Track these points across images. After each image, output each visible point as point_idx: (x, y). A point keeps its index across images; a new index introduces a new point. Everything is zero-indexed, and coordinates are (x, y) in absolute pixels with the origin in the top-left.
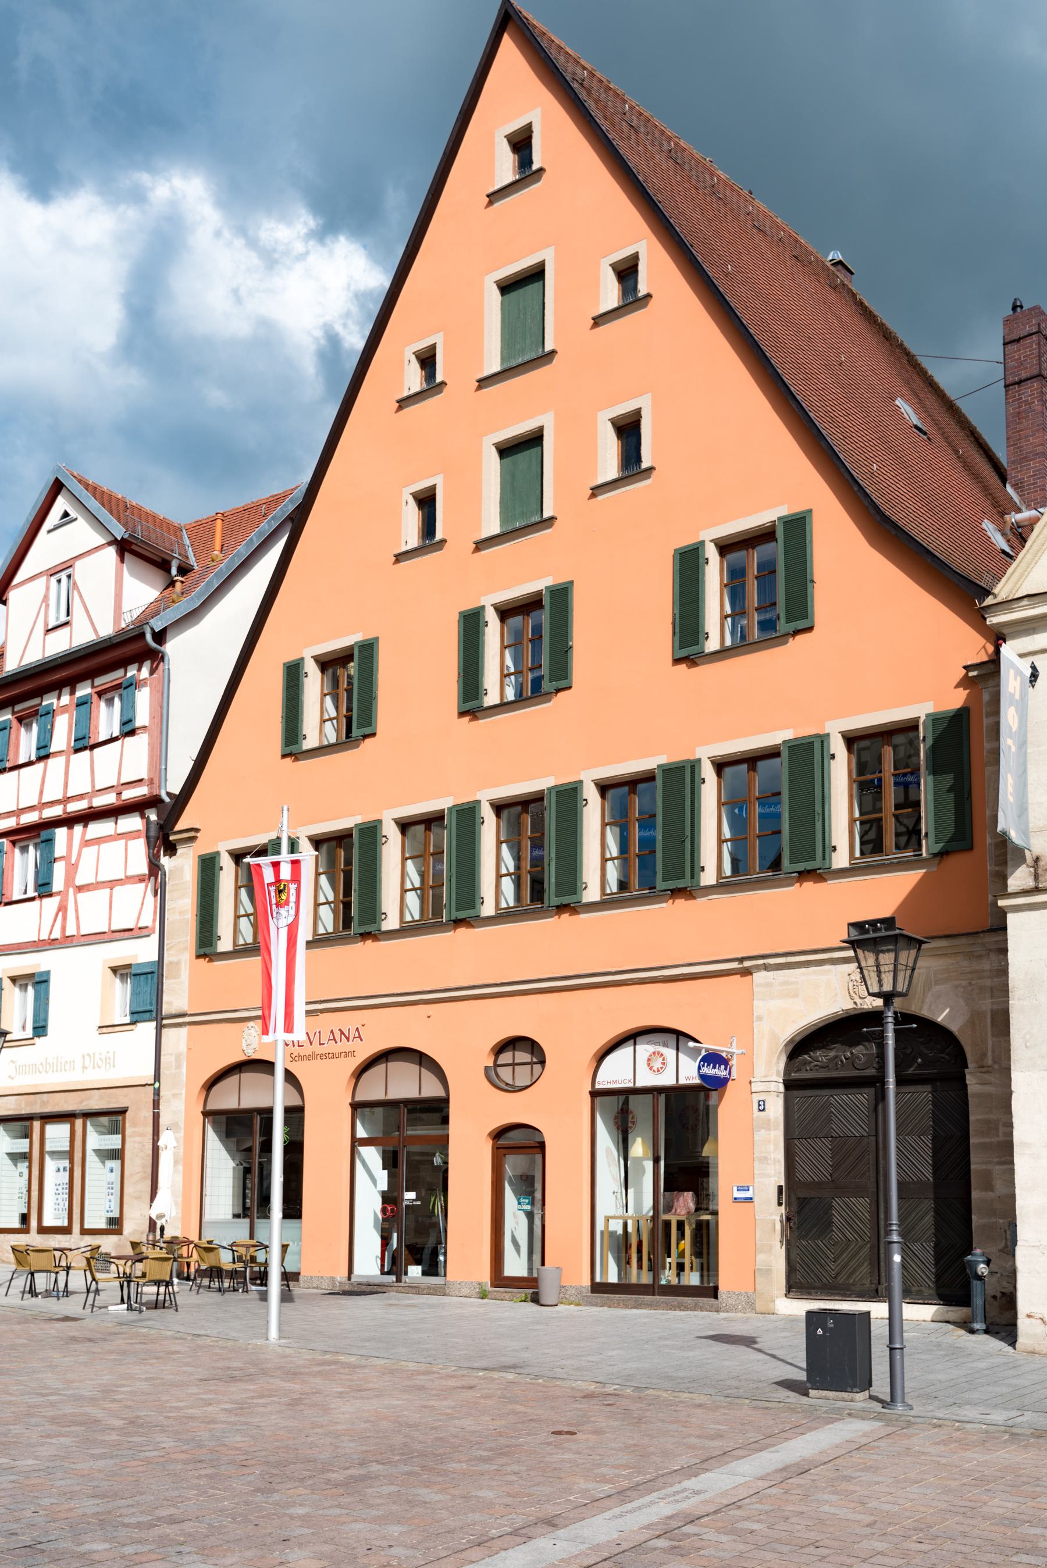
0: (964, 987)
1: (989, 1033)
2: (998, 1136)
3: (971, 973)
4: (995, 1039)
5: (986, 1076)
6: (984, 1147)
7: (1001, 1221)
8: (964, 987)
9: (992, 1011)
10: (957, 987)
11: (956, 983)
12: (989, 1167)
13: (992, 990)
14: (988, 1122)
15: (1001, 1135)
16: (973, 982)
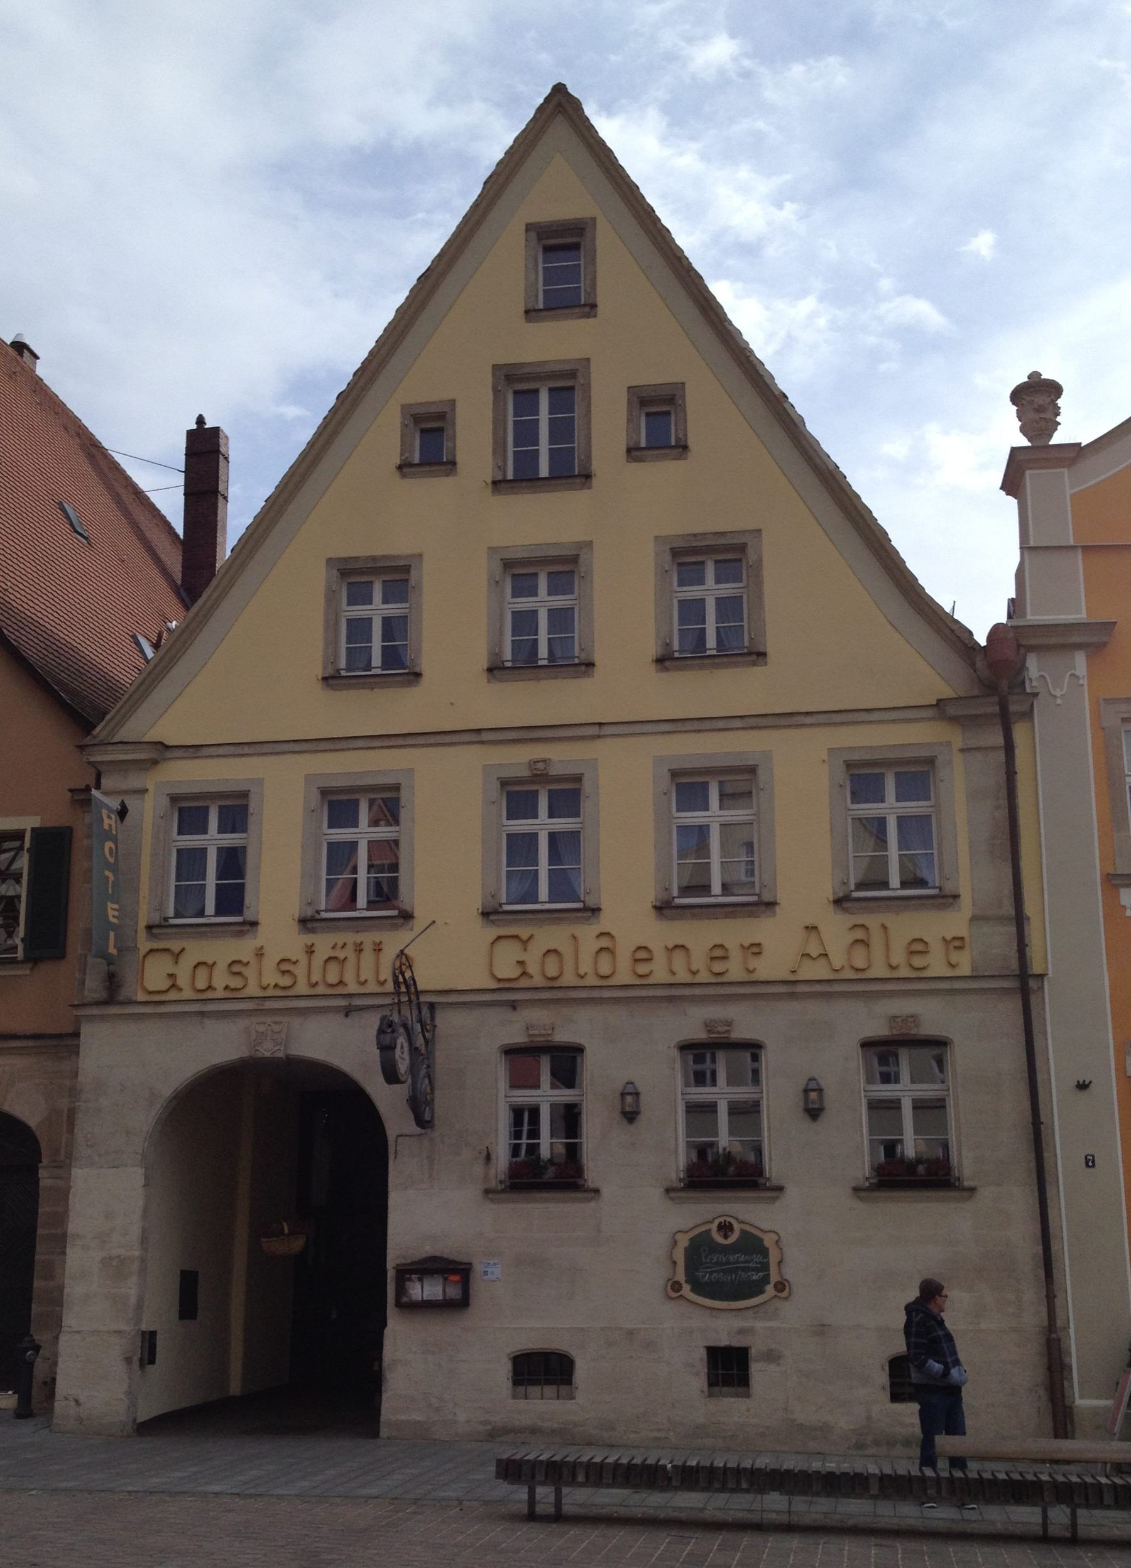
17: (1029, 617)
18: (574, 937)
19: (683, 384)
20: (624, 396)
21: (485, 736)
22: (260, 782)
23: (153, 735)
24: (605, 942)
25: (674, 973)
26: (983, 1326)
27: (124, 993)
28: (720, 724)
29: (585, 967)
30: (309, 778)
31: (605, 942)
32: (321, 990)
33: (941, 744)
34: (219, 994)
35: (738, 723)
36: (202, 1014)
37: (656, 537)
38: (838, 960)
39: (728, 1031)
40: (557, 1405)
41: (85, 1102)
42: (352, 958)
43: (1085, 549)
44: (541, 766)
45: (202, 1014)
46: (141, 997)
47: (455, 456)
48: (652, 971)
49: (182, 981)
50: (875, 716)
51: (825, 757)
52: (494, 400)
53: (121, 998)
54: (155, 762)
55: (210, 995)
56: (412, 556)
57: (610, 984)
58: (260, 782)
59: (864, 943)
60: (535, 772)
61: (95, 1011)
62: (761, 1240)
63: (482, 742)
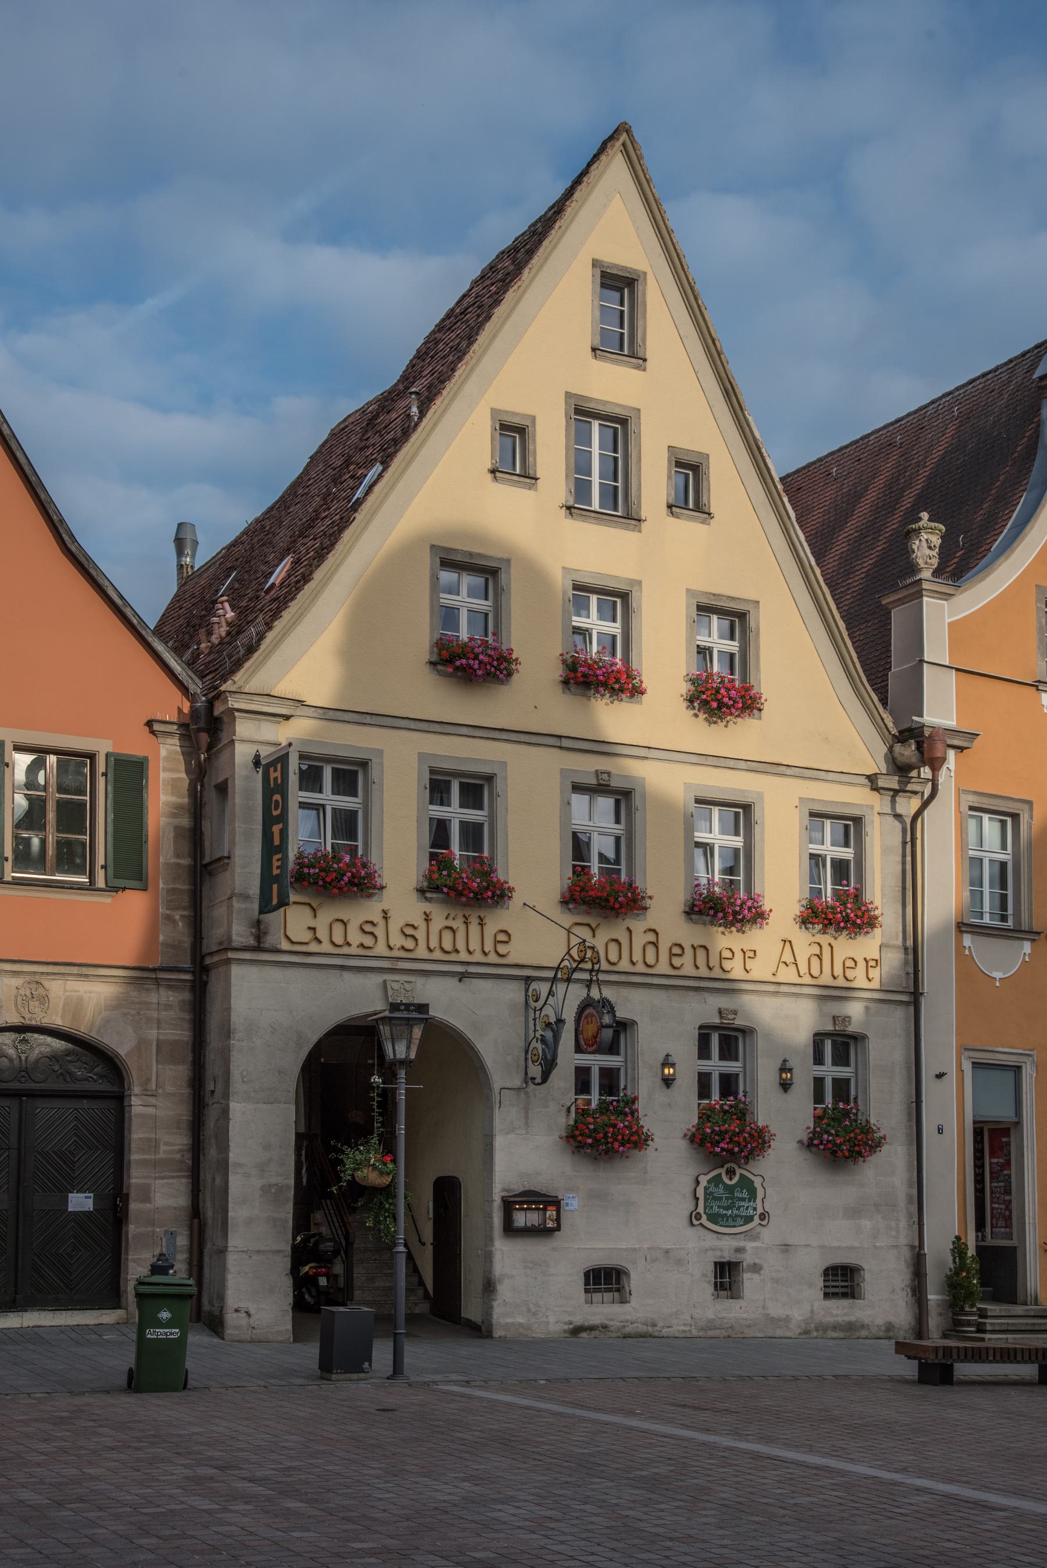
0: (133, 1016)
1: (154, 1061)
2: (159, 1153)
3: (140, 1003)
4: (159, 1066)
5: (151, 1100)
6: (144, 1163)
7: (158, 1230)
8: (133, 1016)
9: (158, 1040)
10: (126, 1014)
11: (126, 1011)
12: (148, 1181)
13: (159, 1022)
14: (149, 1140)
15: (161, 1152)
16: (142, 1013)
17: (925, 717)
18: (629, 930)
19: (708, 455)
20: (665, 455)
21: (566, 743)
22: (380, 752)
23: (282, 688)
24: (651, 937)
25: (697, 967)
26: (878, 1244)
27: (269, 941)
28: (731, 764)
29: (637, 956)
30: (422, 757)
31: (651, 937)
32: (438, 955)
33: (867, 806)
34: (353, 950)
35: (743, 765)
36: (343, 968)
37: (687, 590)
38: (804, 969)
39: (734, 1019)
40: (617, 1308)
41: (239, 1040)
42: (463, 927)
43: (957, 670)
44: (605, 777)
45: (343, 968)
46: (285, 945)
47: (535, 471)
48: (682, 965)
49: (322, 934)
50: (831, 776)
51: (797, 804)
52: (566, 426)
53: (267, 946)
54: (287, 718)
55: (345, 950)
56: (501, 560)
57: (654, 973)
58: (380, 752)
59: (820, 957)
60: (602, 782)
61: (247, 956)
62: (753, 1182)
63: (561, 748)
